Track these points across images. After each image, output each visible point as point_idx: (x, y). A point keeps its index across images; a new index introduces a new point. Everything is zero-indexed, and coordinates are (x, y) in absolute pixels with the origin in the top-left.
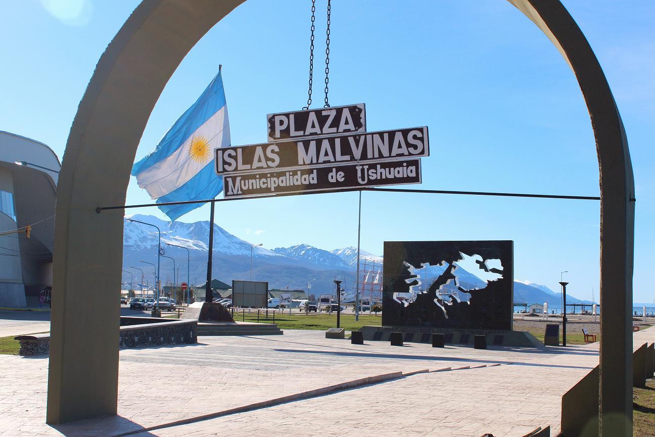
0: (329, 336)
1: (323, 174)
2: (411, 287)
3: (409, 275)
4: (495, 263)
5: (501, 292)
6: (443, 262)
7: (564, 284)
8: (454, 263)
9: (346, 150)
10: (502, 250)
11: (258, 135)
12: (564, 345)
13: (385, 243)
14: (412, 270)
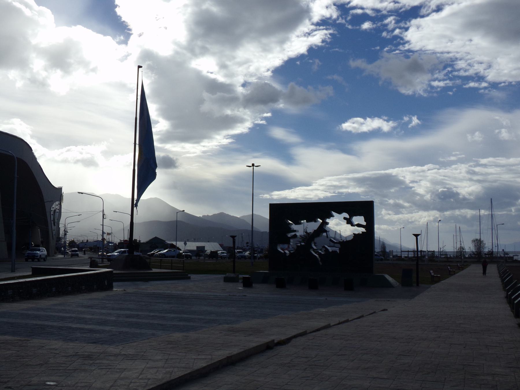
0: (227, 280)
2: (292, 240)
4: (359, 220)
6: (319, 219)
7: (416, 236)
8: (328, 220)
10: (364, 209)
12: (418, 285)
14: (294, 227)
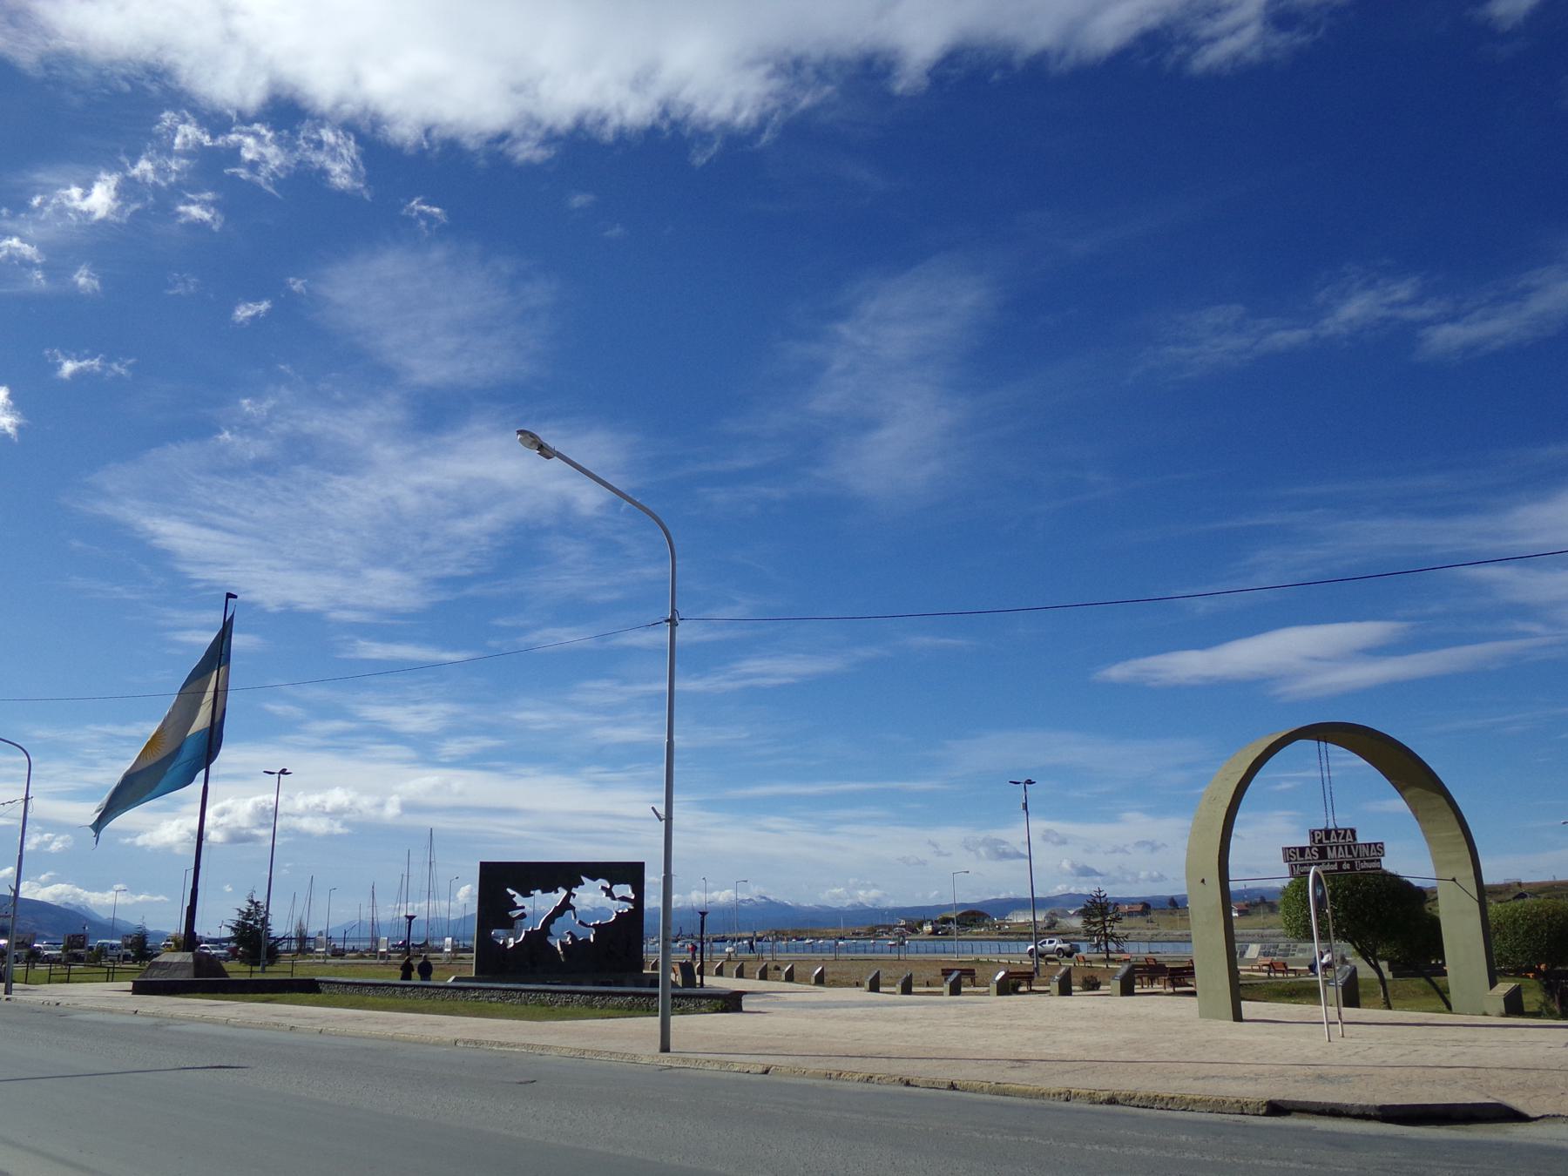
1: (1340, 864)
3: (514, 907)
4: (625, 890)
5: (631, 924)
8: (574, 891)
9: (1350, 852)
10: (631, 873)
11: (1305, 842)
13: (482, 864)
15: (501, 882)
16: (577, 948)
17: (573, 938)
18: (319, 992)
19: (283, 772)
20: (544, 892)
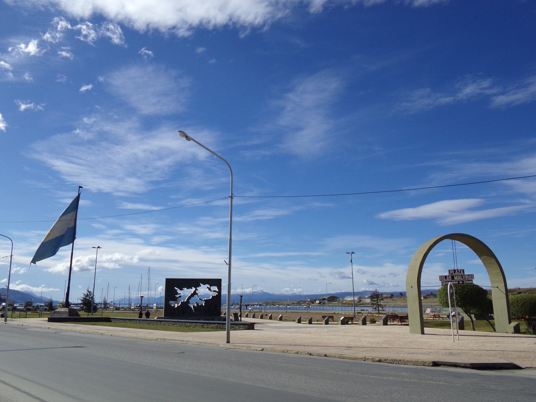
1: (459, 282)
3: (177, 293)
4: (215, 288)
5: (217, 300)
8: (198, 288)
9: (462, 278)
10: (217, 282)
13: (167, 280)
14: (179, 291)
15: (173, 285)
16: (199, 308)
17: (197, 304)
18: (111, 322)
19: (99, 247)
20: (187, 288)
